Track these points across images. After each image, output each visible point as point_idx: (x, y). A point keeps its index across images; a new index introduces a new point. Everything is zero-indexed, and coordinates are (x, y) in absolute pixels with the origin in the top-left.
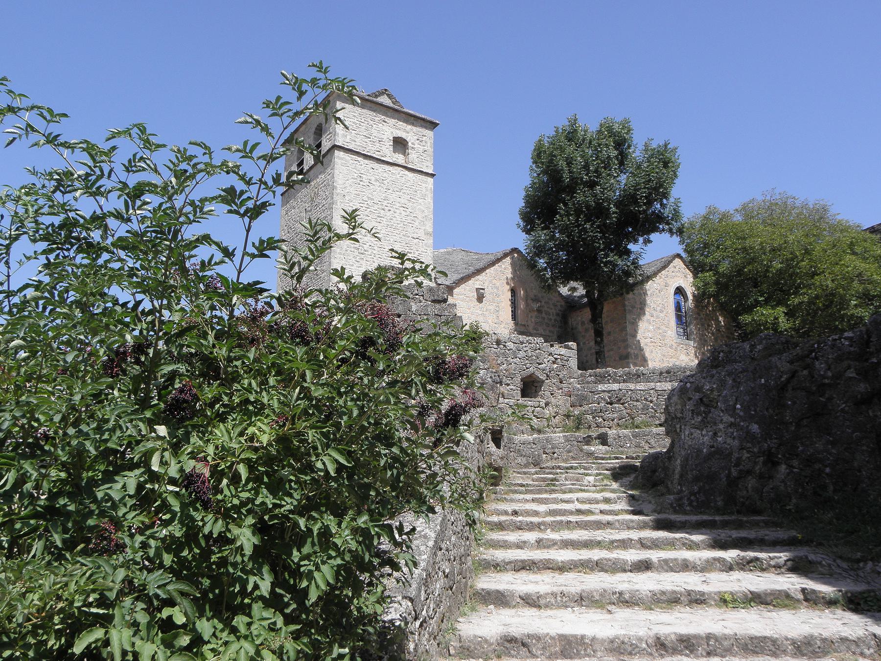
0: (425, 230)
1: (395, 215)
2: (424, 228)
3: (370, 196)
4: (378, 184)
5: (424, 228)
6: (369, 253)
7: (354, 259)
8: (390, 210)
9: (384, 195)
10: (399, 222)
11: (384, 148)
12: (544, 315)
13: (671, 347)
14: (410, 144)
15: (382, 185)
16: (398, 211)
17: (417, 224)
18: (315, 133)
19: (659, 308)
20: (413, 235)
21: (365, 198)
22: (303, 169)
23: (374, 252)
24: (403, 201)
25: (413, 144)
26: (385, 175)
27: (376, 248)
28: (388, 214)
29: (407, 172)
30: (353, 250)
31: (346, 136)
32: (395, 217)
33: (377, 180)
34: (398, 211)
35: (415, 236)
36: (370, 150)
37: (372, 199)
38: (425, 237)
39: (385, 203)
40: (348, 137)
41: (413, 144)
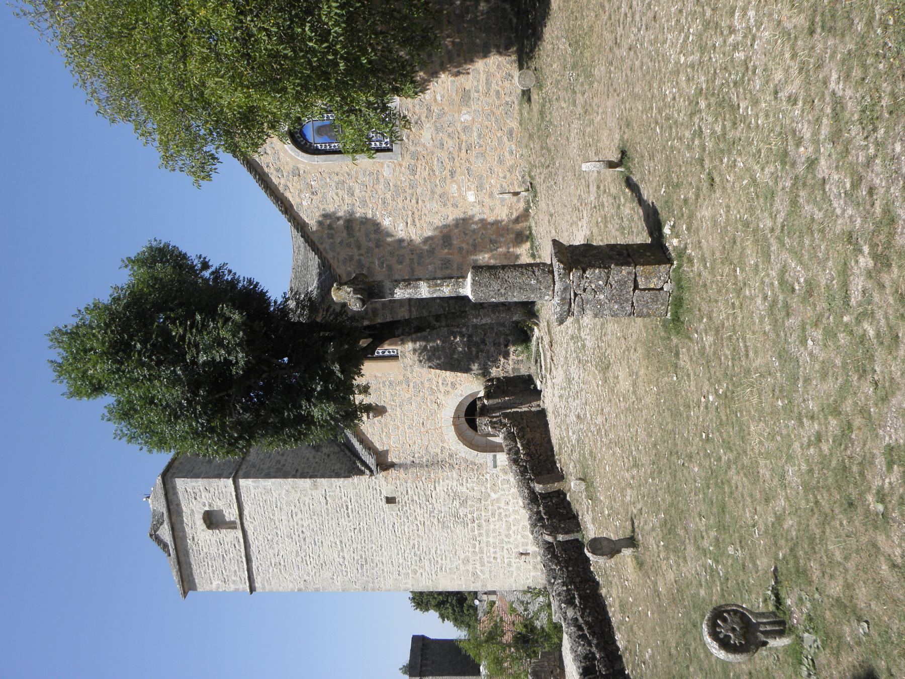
2: (309, 491)
3: (294, 554)
5: (309, 491)
6: (363, 553)
8: (302, 532)
10: (313, 522)
15: (275, 541)
21: (299, 559)
23: (359, 548)
24: (284, 518)
26: (260, 538)
28: (307, 534)
30: (365, 570)
32: (309, 526)
34: (300, 522)
39: (295, 537)
40: (234, 578)
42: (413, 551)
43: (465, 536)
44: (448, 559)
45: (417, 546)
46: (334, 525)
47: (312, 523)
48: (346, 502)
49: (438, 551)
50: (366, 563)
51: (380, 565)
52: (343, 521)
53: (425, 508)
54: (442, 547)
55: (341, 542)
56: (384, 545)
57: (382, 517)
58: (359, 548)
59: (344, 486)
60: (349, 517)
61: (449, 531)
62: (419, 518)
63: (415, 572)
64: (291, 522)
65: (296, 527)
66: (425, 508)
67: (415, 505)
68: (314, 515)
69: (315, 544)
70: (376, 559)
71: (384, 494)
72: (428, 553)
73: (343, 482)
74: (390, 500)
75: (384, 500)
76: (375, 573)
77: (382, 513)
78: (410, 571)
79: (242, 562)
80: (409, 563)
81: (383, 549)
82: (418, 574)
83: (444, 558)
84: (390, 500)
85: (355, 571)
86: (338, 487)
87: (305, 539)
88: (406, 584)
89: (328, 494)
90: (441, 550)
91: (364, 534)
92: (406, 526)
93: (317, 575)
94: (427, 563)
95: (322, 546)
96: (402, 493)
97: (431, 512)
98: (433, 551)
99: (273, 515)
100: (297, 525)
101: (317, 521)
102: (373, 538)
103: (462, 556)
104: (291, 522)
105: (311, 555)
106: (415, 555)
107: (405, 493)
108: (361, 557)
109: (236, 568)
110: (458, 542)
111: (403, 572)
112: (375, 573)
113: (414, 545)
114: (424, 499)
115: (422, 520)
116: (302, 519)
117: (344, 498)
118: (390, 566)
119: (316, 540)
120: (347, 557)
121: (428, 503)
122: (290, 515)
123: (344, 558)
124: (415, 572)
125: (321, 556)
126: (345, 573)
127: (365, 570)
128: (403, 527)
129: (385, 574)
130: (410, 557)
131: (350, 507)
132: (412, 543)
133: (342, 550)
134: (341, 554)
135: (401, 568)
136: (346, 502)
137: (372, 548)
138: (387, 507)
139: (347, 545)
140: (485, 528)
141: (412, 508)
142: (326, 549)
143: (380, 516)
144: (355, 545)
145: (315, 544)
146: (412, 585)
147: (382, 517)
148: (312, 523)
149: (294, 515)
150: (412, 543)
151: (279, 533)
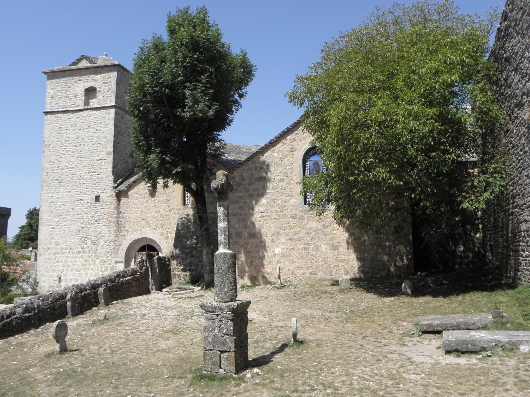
0: (106, 151)
2: (106, 150)
3: (67, 139)
6: (65, 181)
7: (55, 188)
8: (80, 145)
9: (76, 135)
10: (86, 152)
20: (97, 158)
21: (64, 142)
23: (69, 179)
24: (90, 134)
30: (54, 181)
32: (84, 149)
34: (86, 144)
35: (99, 158)
38: (107, 156)
39: (77, 141)
42: (65, 211)
43: (73, 243)
44: (59, 233)
45: (68, 213)
46: (83, 164)
47: (85, 151)
48: (98, 172)
49: (64, 227)
50: (59, 183)
51: (57, 191)
52: (86, 169)
53: (92, 219)
54: (67, 229)
55: (73, 168)
56: (70, 194)
57: (87, 193)
58: (69, 179)
59: (107, 171)
60: (88, 173)
61: (77, 234)
62: (85, 215)
63: (52, 212)
64: (87, 139)
65: (84, 141)
66: (92, 219)
67: (94, 213)
68: (90, 152)
69: (72, 152)
70: (61, 189)
71: (102, 195)
72: (63, 220)
73: (110, 170)
74: (97, 198)
75: (98, 195)
76: (52, 188)
77: (90, 193)
78: (52, 209)
79: (64, 108)
80: (57, 209)
81: (67, 193)
82: (50, 214)
83: (60, 230)
84: (97, 198)
85: (54, 176)
86: (107, 167)
87: (76, 146)
88: (45, 206)
89: (103, 161)
90: (65, 228)
91: (77, 182)
92: (81, 207)
93: (53, 153)
94: (57, 220)
95: (71, 156)
96: (101, 205)
97: (89, 223)
98: (64, 223)
99: (92, 128)
100: (85, 142)
101: (87, 154)
102: (74, 187)
103: (60, 241)
104: (87, 139)
105: (66, 149)
106: (63, 212)
107: (102, 207)
108: (63, 180)
109: (60, 104)
110: (69, 239)
111: (52, 205)
112: (52, 188)
113: (69, 212)
114: (97, 219)
115: (84, 217)
116: (88, 145)
117: (100, 170)
118: (57, 197)
119: (75, 153)
120: (63, 171)
121: (95, 221)
122: (91, 138)
123: (63, 169)
125: (65, 156)
126: (53, 169)
127: (54, 181)
128: (81, 205)
129: (51, 194)
130: (62, 209)
131: (95, 174)
132: (70, 210)
133: (68, 168)
134: (65, 168)
135: (54, 203)
136: (98, 172)
137: (68, 186)
138: (94, 196)
139: (71, 171)
140: (78, 255)
141: (92, 211)
142: (69, 158)
143: (88, 192)
144: (70, 176)
145: (72, 152)
146: (43, 210)
147: (87, 193)
148: (85, 151)
149: (91, 140)
150: (70, 210)
151: (81, 131)
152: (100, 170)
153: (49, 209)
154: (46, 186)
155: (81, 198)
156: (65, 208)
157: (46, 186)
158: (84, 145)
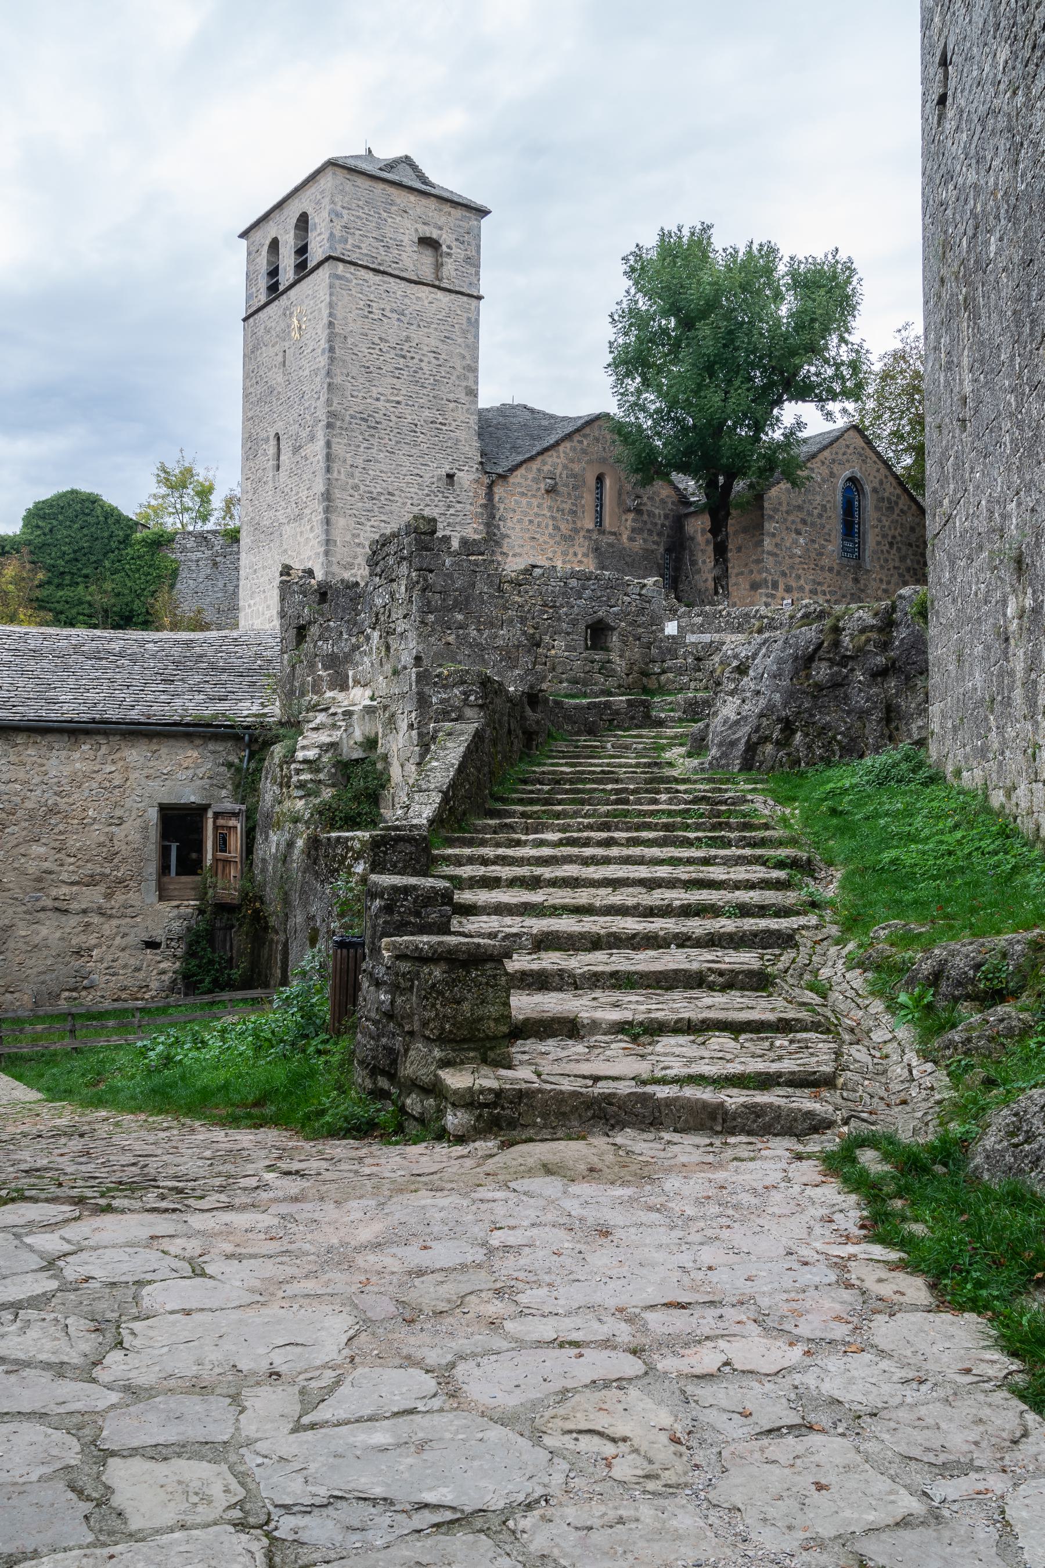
1: (423, 364)
2: (465, 384)
3: (383, 336)
4: (395, 316)
11: (404, 256)
12: (645, 517)
13: (831, 570)
14: (444, 248)
16: (426, 359)
17: (454, 378)
18: (297, 227)
19: (816, 512)
21: (377, 340)
22: (277, 283)
25: (449, 247)
26: (407, 301)
27: (393, 418)
29: (440, 294)
31: (346, 241)
33: (393, 311)
35: (451, 396)
36: (384, 259)
37: (386, 341)
40: (350, 241)
41: (449, 247)
52: (427, 413)
55: (398, 403)
64: (426, 348)
75: (451, 472)
82: (351, 492)
84: (450, 476)
87: (404, 357)
104: (426, 348)
109: (365, 251)
117: (454, 424)
118: (364, 457)
120: (379, 404)
123: (378, 399)
124: (356, 488)
133: (388, 401)
138: (443, 472)
144: (393, 418)
152: (454, 424)
153: (350, 481)
154: (341, 428)
155: (416, 471)
156: (384, 485)
157: (341, 428)
158: (421, 361)
